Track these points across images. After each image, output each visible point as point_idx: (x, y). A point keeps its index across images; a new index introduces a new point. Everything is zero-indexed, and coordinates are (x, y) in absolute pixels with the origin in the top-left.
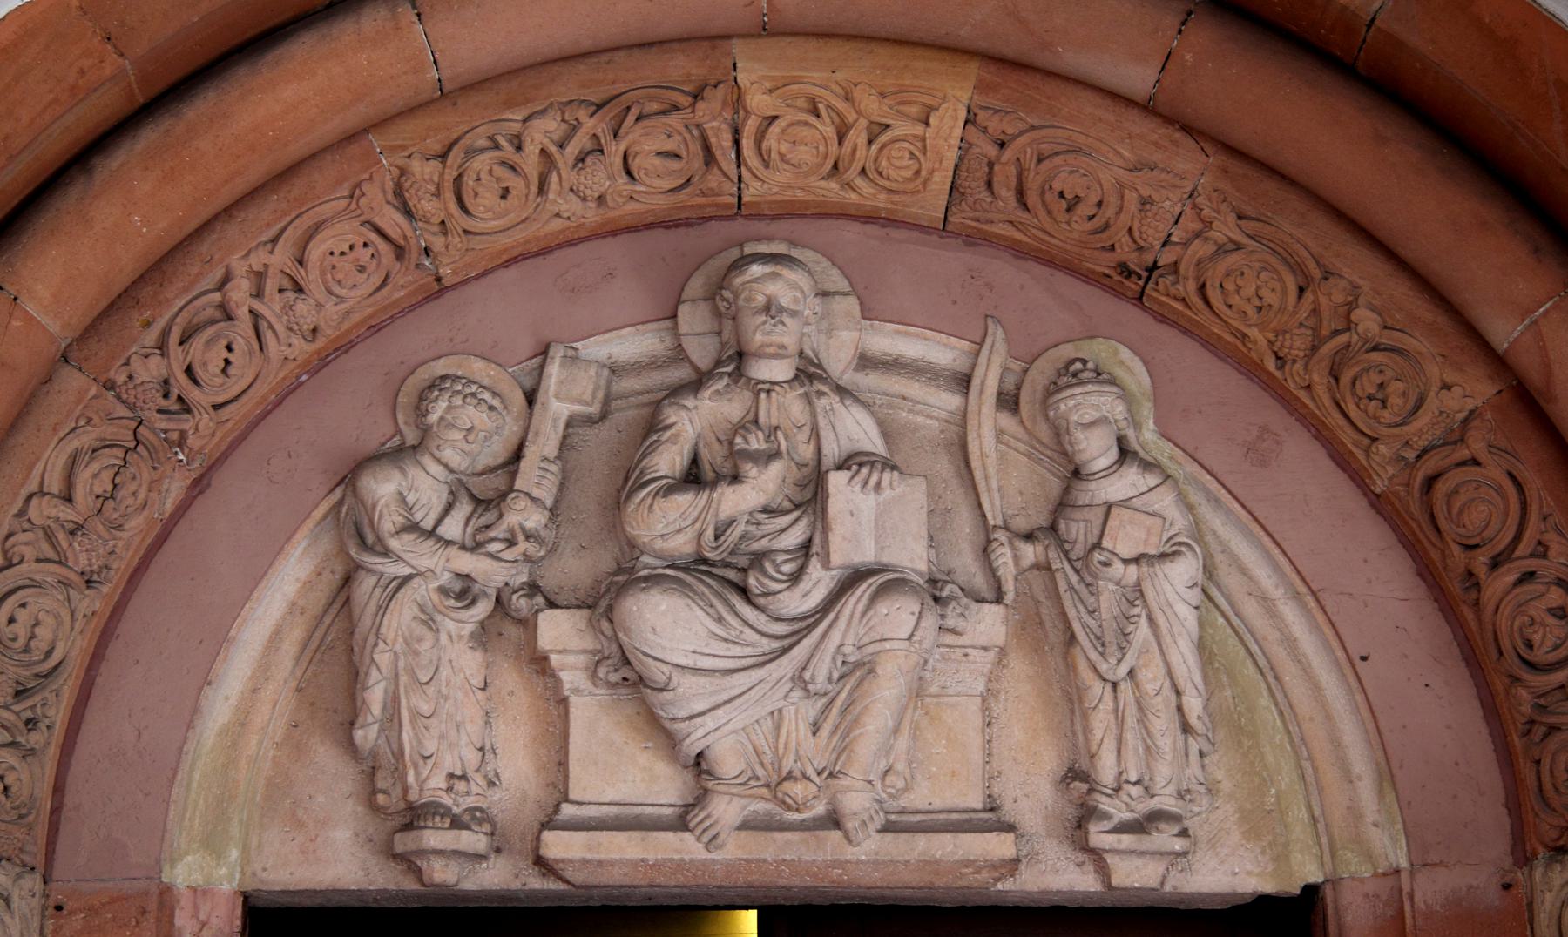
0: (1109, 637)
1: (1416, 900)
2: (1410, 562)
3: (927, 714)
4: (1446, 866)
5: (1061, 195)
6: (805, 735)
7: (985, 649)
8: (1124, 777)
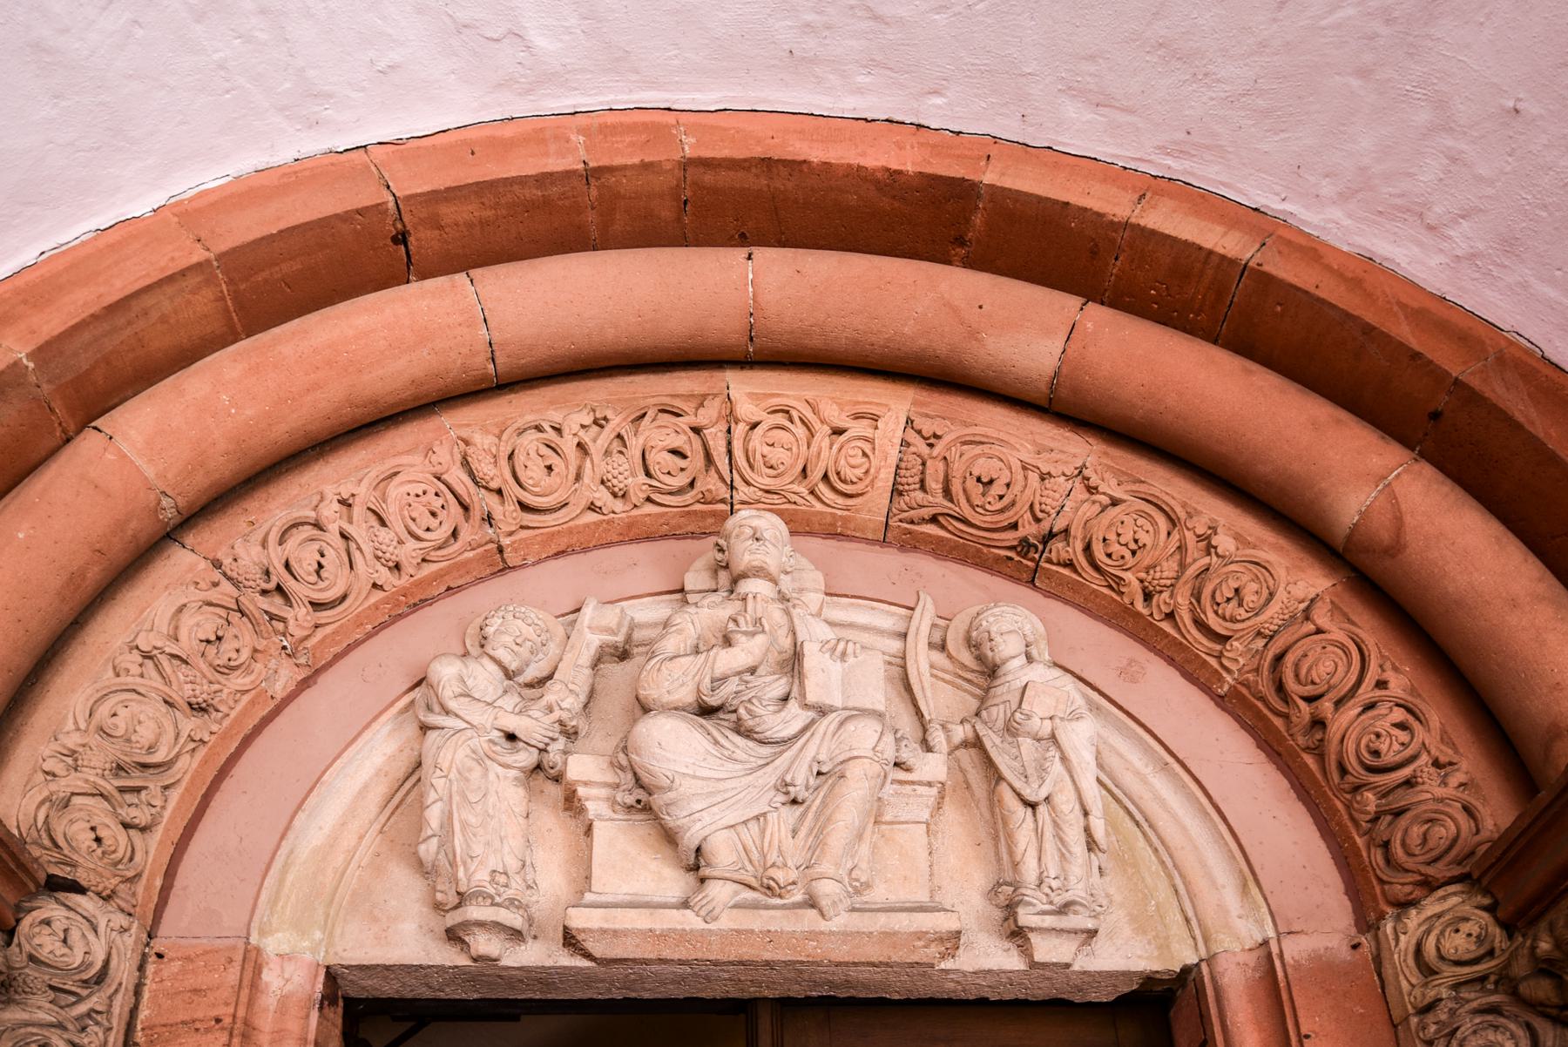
0: (1030, 771)
1: (1285, 956)
2: (1252, 740)
3: (883, 836)
4: (1306, 934)
5: (979, 480)
6: (787, 836)
7: (930, 784)
8: (1045, 874)
